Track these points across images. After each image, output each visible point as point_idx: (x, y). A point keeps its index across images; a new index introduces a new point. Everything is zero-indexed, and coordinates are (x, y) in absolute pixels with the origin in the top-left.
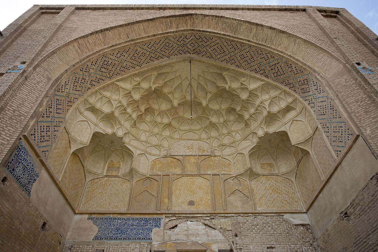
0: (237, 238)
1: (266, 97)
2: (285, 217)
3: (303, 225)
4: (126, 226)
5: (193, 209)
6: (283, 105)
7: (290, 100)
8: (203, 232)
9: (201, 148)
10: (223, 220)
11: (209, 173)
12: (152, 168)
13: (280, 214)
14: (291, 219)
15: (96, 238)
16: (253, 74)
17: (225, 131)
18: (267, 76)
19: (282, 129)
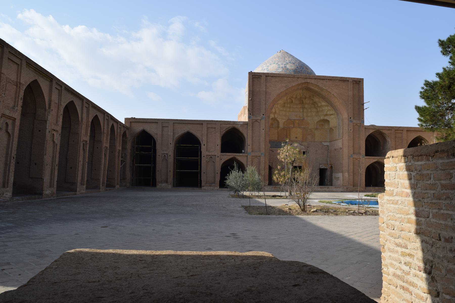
0: (308, 148)
1: (327, 108)
2: (323, 143)
3: (327, 145)
4: (278, 144)
5: (297, 139)
6: (331, 113)
7: (333, 112)
8: (299, 146)
9: (300, 116)
10: (305, 143)
11: (302, 127)
12: (284, 125)
13: (321, 142)
14: (324, 144)
15: (270, 147)
16: (324, 101)
17: (309, 111)
18: (328, 104)
19: (329, 120)
